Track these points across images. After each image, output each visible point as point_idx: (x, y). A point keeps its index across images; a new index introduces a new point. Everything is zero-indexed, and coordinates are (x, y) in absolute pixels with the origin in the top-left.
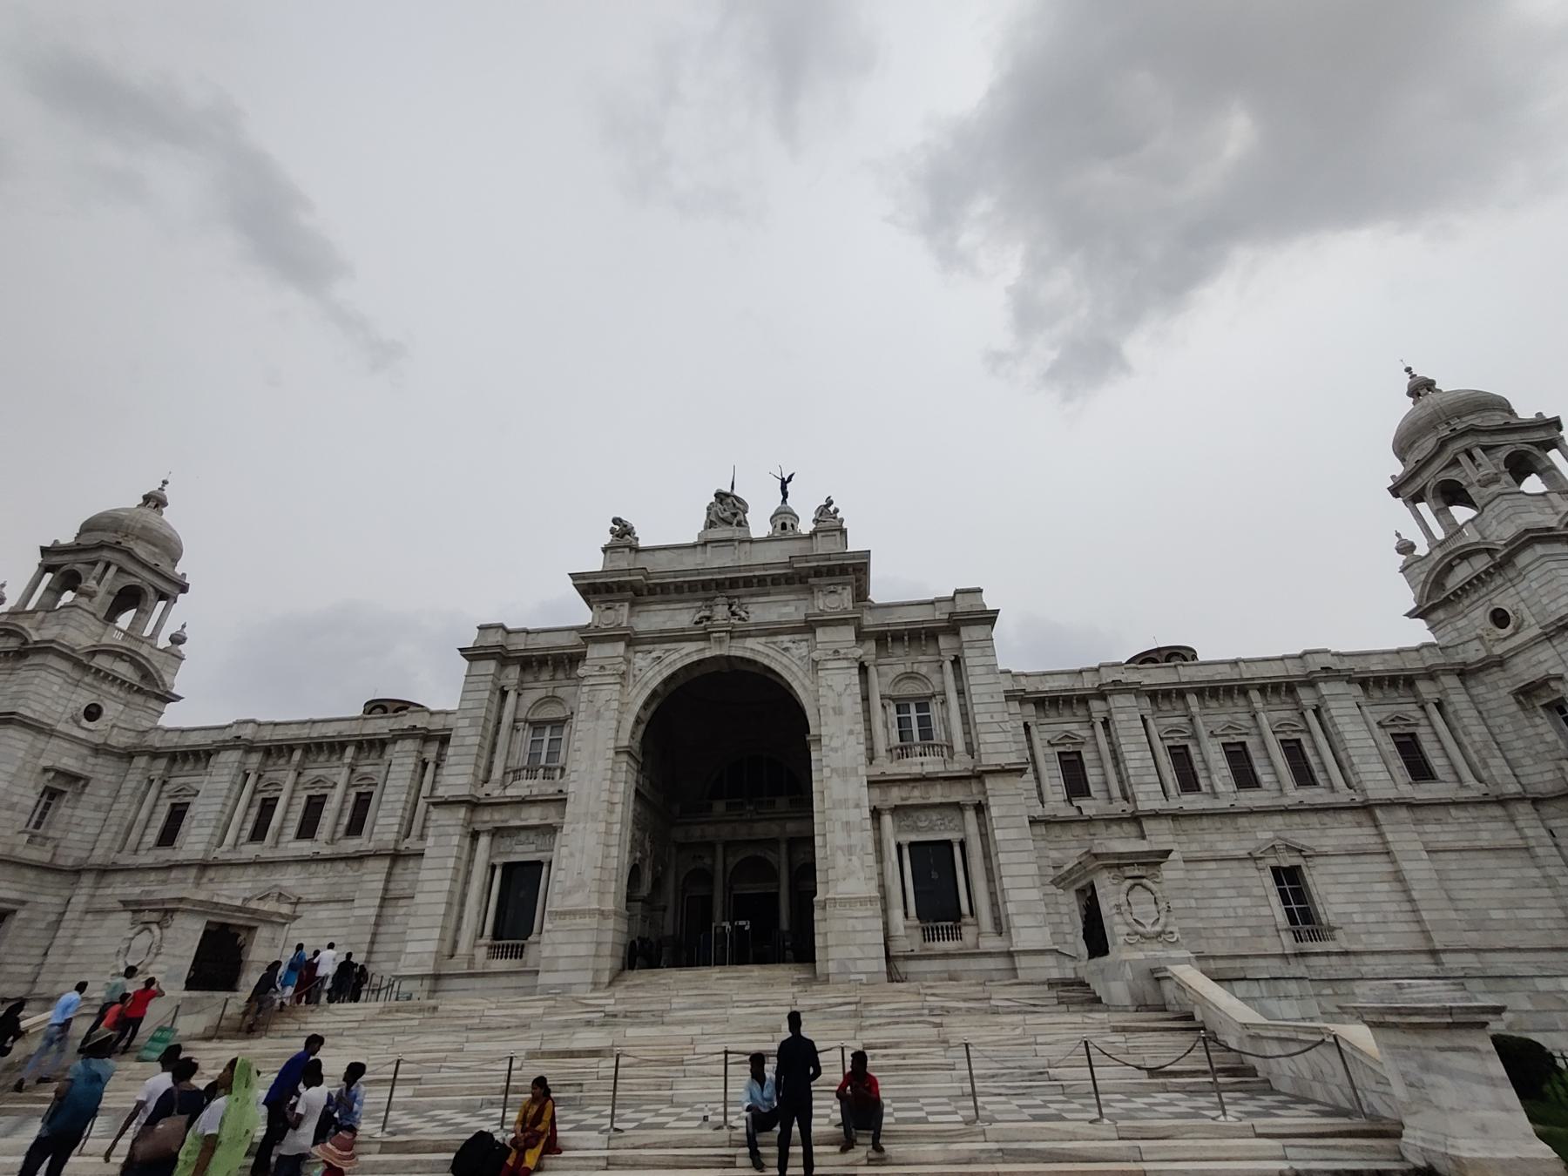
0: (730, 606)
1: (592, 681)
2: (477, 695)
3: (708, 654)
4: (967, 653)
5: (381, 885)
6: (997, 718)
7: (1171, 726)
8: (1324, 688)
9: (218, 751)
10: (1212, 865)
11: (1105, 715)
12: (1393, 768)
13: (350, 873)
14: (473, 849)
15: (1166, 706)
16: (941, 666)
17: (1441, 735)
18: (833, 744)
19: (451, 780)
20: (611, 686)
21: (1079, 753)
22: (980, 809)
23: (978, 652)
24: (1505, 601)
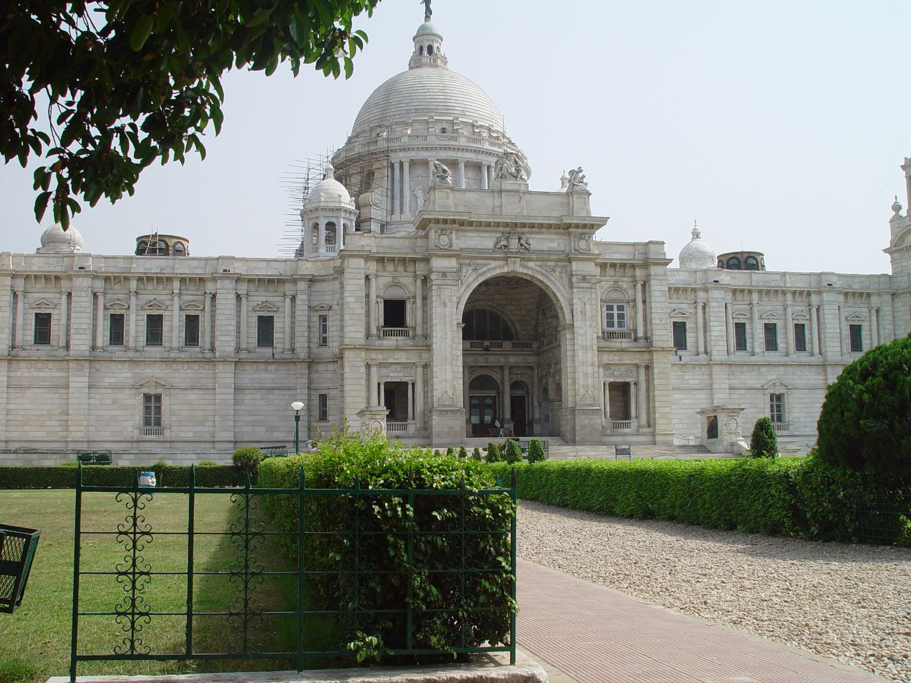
0: (520, 239)
1: (437, 282)
2: (357, 282)
3: (506, 270)
4: (653, 282)
5: (232, 381)
6: (663, 322)
7: (740, 310)
8: (825, 296)
9: (70, 278)
10: (742, 392)
11: (704, 301)
12: (844, 345)
13: (204, 371)
14: (368, 374)
15: (739, 297)
16: (635, 286)
17: (872, 330)
19: (352, 335)
20: (451, 287)
21: (684, 323)
22: (647, 367)
23: (658, 282)
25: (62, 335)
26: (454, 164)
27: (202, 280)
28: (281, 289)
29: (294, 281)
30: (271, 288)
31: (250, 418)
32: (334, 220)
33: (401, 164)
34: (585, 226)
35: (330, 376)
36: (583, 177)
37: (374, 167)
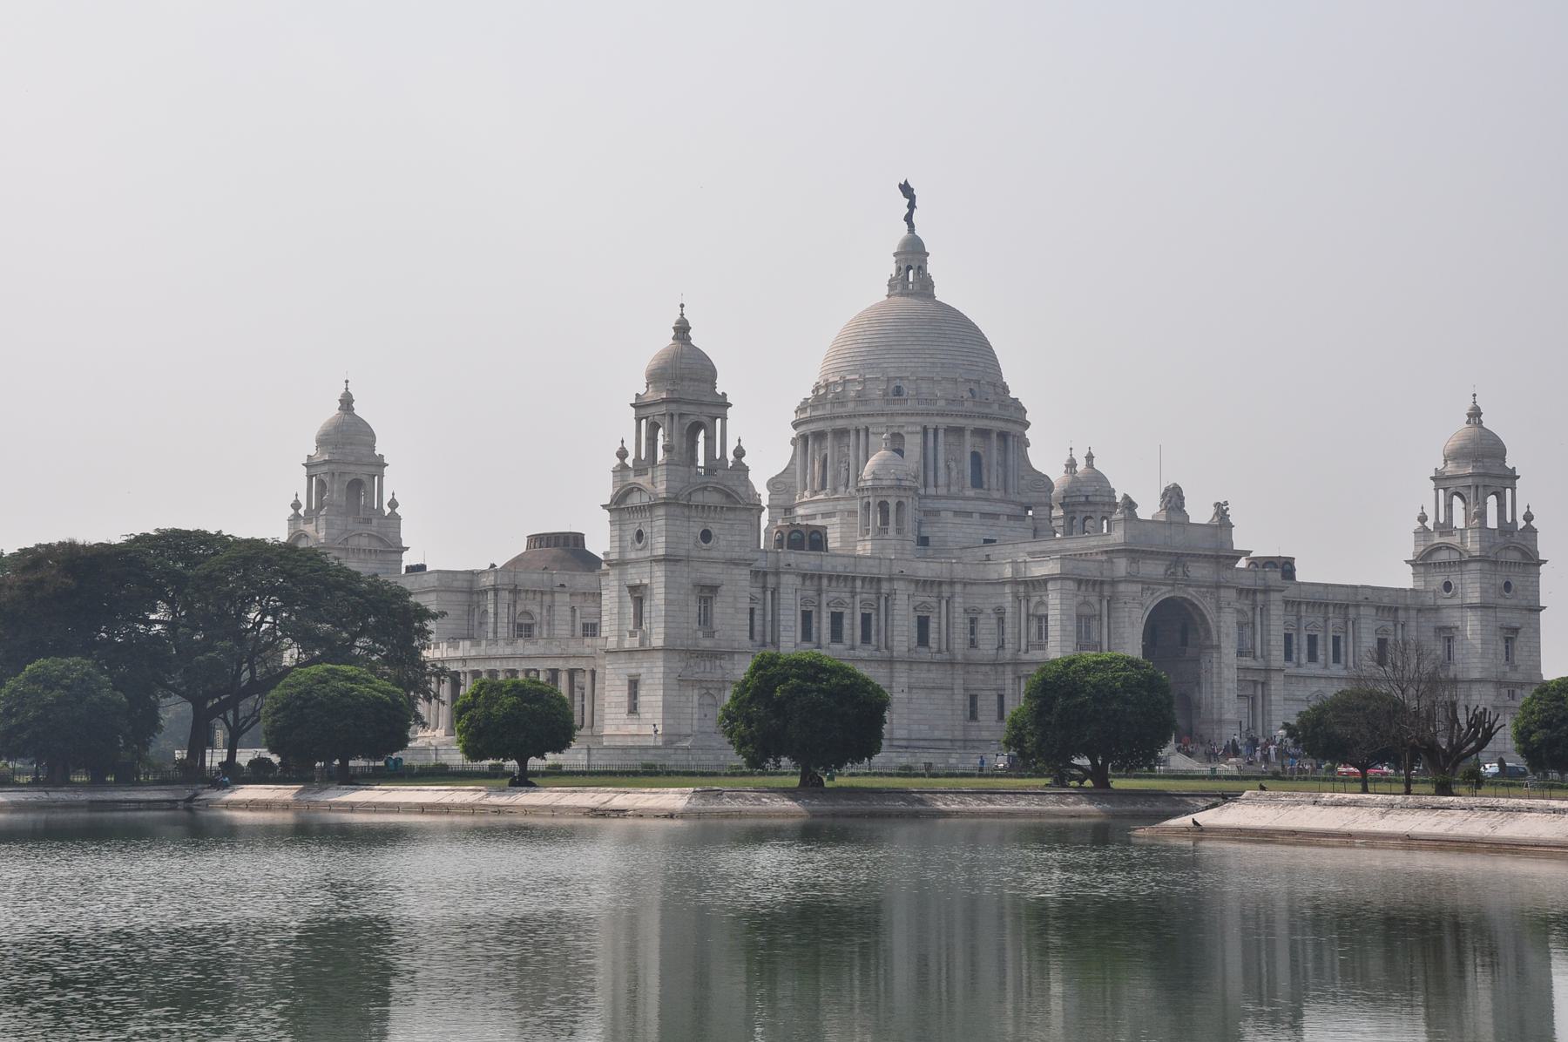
0: (1184, 565)
4: (1272, 607)
10: (1291, 702)
16: (1254, 609)
18: (1226, 652)
24: (1454, 580)
25: (769, 629)
26: (984, 433)
27: (879, 580)
28: (936, 589)
29: (952, 583)
30: (928, 589)
31: (915, 717)
32: (904, 500)
33: (936, 430)
34: (1233, 557)
35: (981, 677)
36: (1228, 509)
37: (906, 429)
